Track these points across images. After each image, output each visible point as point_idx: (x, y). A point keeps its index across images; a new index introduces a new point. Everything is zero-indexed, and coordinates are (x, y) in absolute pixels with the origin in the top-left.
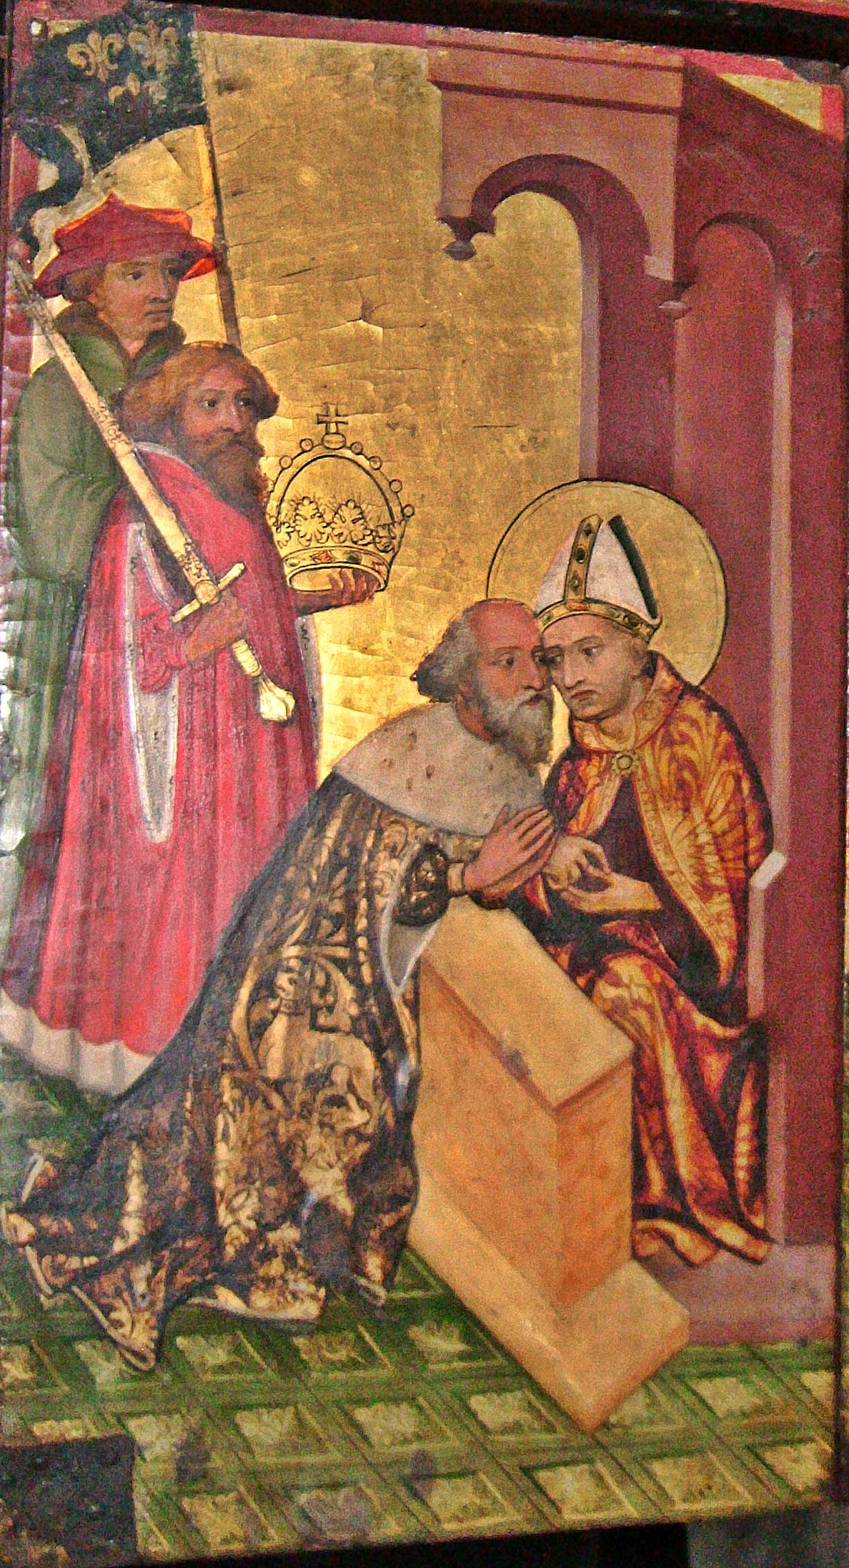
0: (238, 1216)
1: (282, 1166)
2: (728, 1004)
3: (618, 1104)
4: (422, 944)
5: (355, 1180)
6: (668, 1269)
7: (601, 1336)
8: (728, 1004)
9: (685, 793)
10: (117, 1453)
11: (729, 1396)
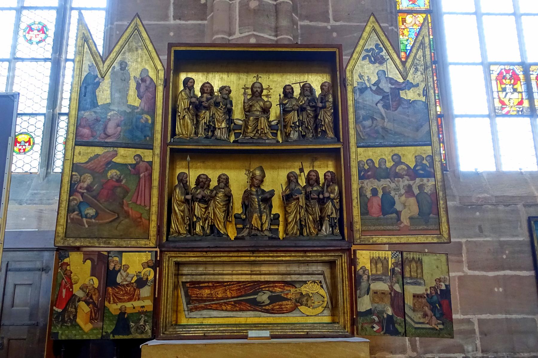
0: (66, 319)
1: (69, 316)
2: (97, 307)
3: (89, 313)
4: (78, 303)
5: (73, 317)
6: (92, 323)
7: (87, 327)
8: (97, 307)
9: (95, 295)
10: (58, 333)
11: (95, 331)
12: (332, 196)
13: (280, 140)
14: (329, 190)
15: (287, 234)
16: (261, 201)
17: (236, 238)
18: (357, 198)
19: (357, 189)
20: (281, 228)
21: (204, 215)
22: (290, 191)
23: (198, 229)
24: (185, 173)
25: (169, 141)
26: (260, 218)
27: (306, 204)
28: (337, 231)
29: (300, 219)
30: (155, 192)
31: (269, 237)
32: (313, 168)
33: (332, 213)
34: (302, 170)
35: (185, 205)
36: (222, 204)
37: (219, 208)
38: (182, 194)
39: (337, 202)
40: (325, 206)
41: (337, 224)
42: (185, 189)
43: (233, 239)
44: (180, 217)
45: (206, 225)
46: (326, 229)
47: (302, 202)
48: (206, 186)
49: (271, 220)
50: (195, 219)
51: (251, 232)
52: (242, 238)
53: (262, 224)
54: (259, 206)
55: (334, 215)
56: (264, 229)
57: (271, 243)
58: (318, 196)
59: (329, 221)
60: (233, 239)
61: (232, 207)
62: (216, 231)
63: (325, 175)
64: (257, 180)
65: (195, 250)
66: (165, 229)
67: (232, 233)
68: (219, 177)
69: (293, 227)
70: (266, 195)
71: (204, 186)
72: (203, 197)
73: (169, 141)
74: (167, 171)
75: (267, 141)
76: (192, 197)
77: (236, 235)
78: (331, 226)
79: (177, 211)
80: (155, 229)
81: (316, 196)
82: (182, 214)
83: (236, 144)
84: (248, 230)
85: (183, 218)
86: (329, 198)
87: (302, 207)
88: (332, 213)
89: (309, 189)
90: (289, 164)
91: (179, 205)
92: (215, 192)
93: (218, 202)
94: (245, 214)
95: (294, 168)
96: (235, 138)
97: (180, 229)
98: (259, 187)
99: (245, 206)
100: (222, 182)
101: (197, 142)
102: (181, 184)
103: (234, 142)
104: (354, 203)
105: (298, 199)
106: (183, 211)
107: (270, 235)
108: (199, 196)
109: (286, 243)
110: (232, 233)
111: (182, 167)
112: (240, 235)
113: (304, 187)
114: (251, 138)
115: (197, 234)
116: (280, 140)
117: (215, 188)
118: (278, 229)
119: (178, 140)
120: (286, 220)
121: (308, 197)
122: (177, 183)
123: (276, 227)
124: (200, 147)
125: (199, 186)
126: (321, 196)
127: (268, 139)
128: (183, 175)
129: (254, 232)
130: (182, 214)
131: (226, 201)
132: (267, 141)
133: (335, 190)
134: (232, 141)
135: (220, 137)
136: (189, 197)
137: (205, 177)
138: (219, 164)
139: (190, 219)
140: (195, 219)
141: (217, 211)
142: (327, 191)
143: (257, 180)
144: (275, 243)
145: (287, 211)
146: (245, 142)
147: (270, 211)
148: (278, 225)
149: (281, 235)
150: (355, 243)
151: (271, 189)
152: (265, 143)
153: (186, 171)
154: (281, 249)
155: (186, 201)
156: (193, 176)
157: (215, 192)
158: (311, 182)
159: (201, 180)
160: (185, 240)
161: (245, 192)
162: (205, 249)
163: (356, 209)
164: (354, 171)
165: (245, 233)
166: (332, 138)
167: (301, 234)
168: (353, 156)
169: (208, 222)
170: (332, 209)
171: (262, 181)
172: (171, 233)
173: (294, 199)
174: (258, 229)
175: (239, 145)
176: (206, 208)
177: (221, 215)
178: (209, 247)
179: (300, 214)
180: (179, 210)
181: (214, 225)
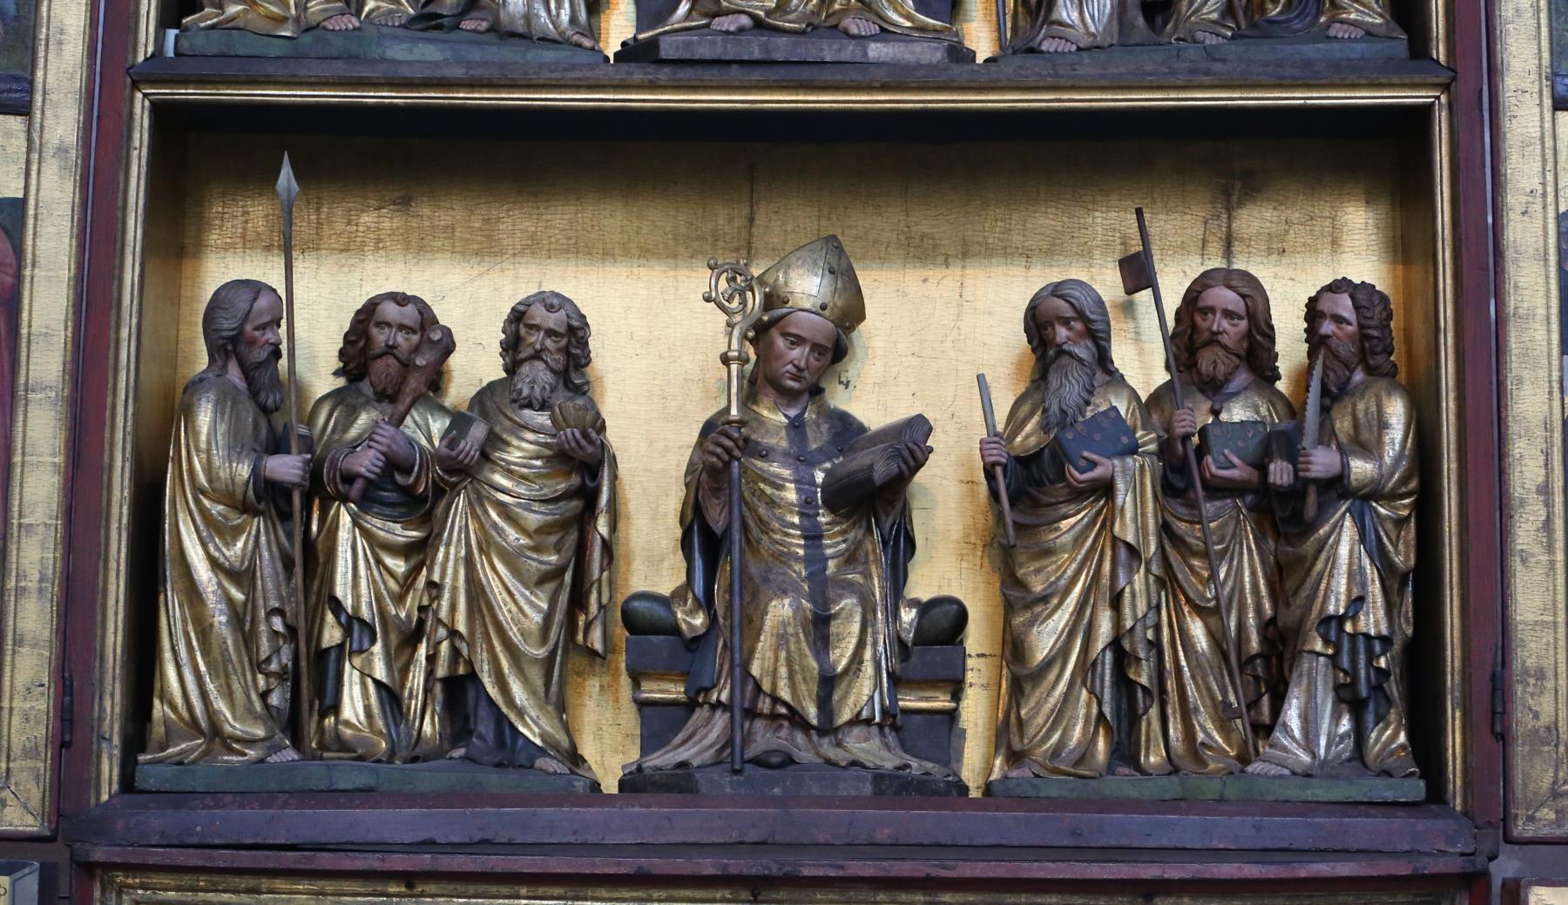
12: (1361, 468)
13: (980, 38)
14: (1343, 425)
15: (1015, 758)
16: (831, 504)
17: (633, 783)
18: (1545, 490)
19: (1547, 427)
20: (976, 710)
21: (399, 599)
22: (1045, 427)
23: (354, 703)
24: (256, 288)
25: (145, 47)
26: (820, 627)
27: (1165, 529)
28: (1390, 737)
29: (1115, 644)
30: (41, 431)
31: (879, 777)
32: (1228, 253)
33: (1356, 603)
34: (1136, 271)
35: (258, 523)
36: (533, 519)
37: (510, 558)
38: (236, 447)
39: (1400, 523)
40: (1309, 546)
41: (1393, 688)
42: (265, 410)
43: (610, 786)
44: (220, 619)
45: (417, 679)
46: (1309, 723)
47: (1135, 510)
48: (414, 383)
49: (902, 648)
50: (332, 634)
51: (747, 740)
52: (680, 782)
53: (828, 683)
54: (813, 537)
55: (1373, 620)
56: (845, 715)
57: (889, 822)
58: (1262, 468)
59: (1334, 659)
60: (610, 786)
61: (607, 547)
62: (485, 727)
63: (1314, 313)
64: (798, 340)
65: (325, 861)
66: (112, 704)
67: (608, 741)
68: (518, 317)
69: (1066, 696)
70: (862, 459)
71: (403, 380)
72: (394, 465)
73: (145, 47)
74: (131, 275)
75: (876, 51)
76: (314, 472)
77: (634, 754)
78: (1349, 699)
79: (203, 572)
80: (41, 705)
81: (1239, 472)
82: (238, 596)
83: (638, 74)
84: (721, 720)
85: (238, 616)
86: (1337, 487)
87: (1133, 552)
88: (1356, 603)
89: (1196, 414)
90: (1046, 220)
91: (214, 529)
92: (478, 431)
93: (502, 508)
94: (707, 603)
95: (1085, 255)
96: (640, 28)
97: (220, 705)
98: (816, 391)
99: (704, 537)
100: (537, 356)
101: (352, 58)
102: (234, 374)
103: (629, 52)
104: (1526, 532)
105: (1105, 489)
106: (242, 576)
107: (889, 761)
108: (366, 462)
109: (1010, 825)
110: (608, 741)
111: (247, 242)
112: (663, 759)
113: (1157, 396)
114: (759, 24)
115: (342, 745)
116: (980, 38)
117: (486, 397)
118: (952, 716)
119: (214, 44)
120: (1013, 648)
121: (1179, 474)
122: (203, 361)
123: (942, 702)
124: (371, 97)
125: (366, 387)
126: (1280, 473)
127: (886, 33)
128: (242, 301)
129: (764, 738)
130: (238, 596)
131: (566, 496)
132: (876, 51)
133: (1383, 425)
134: (612, 47)
135: (528, 17)
136: (287, 467)
137: (409, 314)
138: (516, 220)
139: (292, 630)
140: (332, 634)
141: (497, 578)
142: (1326, 435)
143: (798, 340)
144: (923, 821)
145: (1021, 584)
146: (705, 52)
147: (897, 578)
148: (957, 688)
149: (975, 760)
150: (1522, 829)
151: (901, 411)
152: (865, 65)
153: (269, 272)
154: (966, 870)
155: (268, 498)
156: (321, 305)
157: (478, 431)
158: (1207, 361)
159: (381, 337)
160: (258, 790)
161: (708, 428)
162: (398, 862)
163: (1538, 574)
164: (1532, 288)
165: (698, 744)
166: (1370, 34)
167: (1126, 752)
168: (1523, 171)
169: (432, 659)
170: (1356, 575)
171: (836, 351)
172: (158, 730)
173: (1079, 495)
174: (796, 718)
175: (664, 74)
176: (419, 552)
177: (523, 609)
178: (428, 845)
179: (1116, 603)
180: (215, 564)
181: (473, 676)
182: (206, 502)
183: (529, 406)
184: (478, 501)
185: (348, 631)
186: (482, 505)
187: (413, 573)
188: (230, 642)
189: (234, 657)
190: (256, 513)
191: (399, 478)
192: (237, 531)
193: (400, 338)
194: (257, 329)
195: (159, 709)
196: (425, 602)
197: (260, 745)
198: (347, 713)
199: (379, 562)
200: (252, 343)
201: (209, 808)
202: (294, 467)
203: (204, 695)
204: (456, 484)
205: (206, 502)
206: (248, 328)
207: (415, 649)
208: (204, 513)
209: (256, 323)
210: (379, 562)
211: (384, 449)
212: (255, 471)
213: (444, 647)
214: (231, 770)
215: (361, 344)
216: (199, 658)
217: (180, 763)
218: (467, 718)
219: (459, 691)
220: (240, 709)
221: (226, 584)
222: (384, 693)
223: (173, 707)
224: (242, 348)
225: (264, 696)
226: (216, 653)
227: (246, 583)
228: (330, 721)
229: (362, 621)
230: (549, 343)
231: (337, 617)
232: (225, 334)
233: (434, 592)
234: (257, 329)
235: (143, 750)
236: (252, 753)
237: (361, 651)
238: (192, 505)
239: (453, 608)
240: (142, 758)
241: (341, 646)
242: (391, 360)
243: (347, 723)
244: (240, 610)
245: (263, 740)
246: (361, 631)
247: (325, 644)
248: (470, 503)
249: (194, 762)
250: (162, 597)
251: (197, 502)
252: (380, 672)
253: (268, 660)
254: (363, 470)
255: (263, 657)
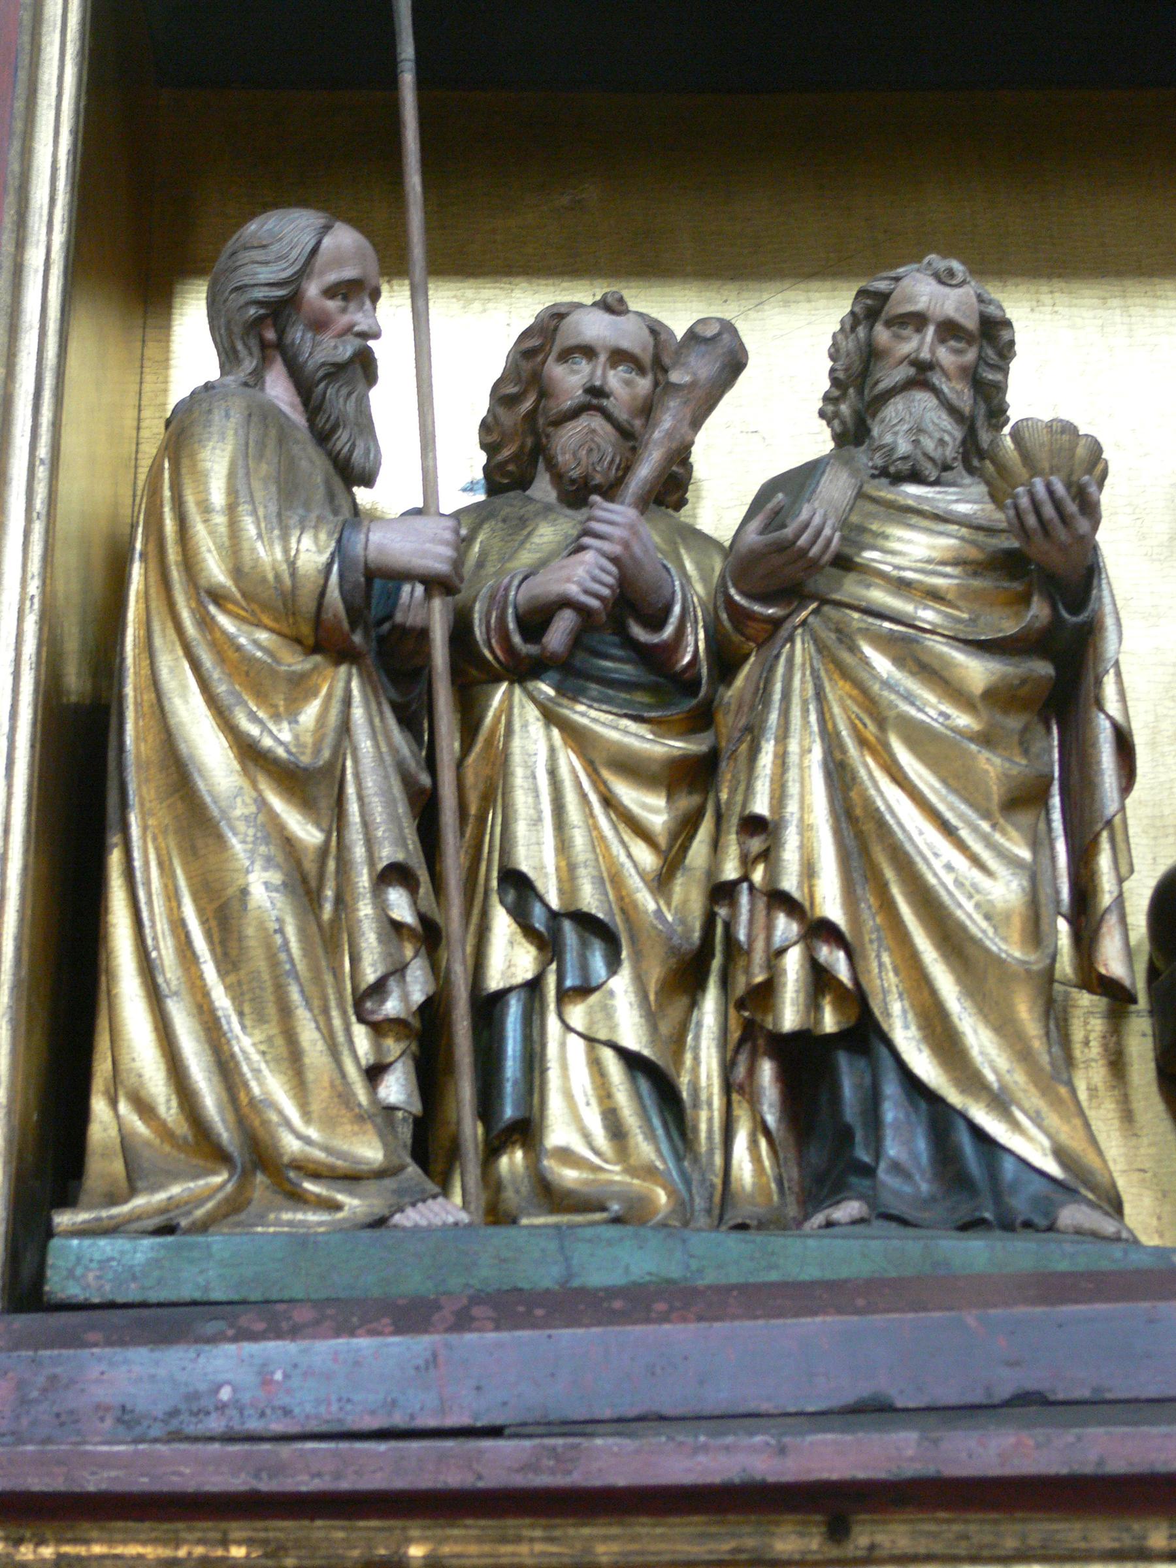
23: (578, 1111)
44: (262, 889)
50: (510, 958)
62: (902, 1143)
85: (305, 883)
91: (235, 682)
97: (270, 1085)
100: (922, 375)
102: (278, 389)
130: (307, 832)
159: (570, 380)
180: (250, 754)
181: (865, 1033)
182: (223, 620)
183: (916, 477)
184: (837, 656)
185: (548, 944)
186: (854, 649)
187: (686, 827)
188: (291, 931)
189: (301, 966)
190: (342, 654)
191: (639, 633)
192: (299, 688)
193: (615, 379)
194: (330, 292)
195: (104, 1119)
196: (730, 871)
197: (372, 1186)
198: (559, 1132)
199: (609, 802)
200: (319, 324)
201: (254, 1337)
202: (434, 540)
203: (226, 1067)
204: (776, 623)
205: (223, 620)
206: (313, 290)
207: (695, 1003)
208: (223, 646)
209: (332, 277)
210: (609, 802)
211: (615, 549)
212: (340, 550)
213: (793, 961)
214: (302, 1241)
215: (527, 405)
216: (209, 971)
217: (169, 1229)
218: (845, 1135)
219: (823, 1077)
220: (320, 1097)
221: (277, 803)
222: (644, 1085)
223: (144, 1108)
224: (298, 334)
225: (374, 1073)
226: (258, 961)
227: (326, 805)
228: (513, 1161)
229: (587, 922)
230: (944, 355)
231: (520, 915)
232: (260, 294)
233: (756, 845)
234: (330, 292)
235: (67, 1199)
236: (353, 1204)
237: (585, 990)
238: (191, 629)
239: (809, 871)
240: (63, 1219)
241: (534, 986)
242: (596, 422)
243: (566, 1155)
244: (310, 866)
245: (380, 1174)
246: (584, 945)
247: (495, 981)
248: (821, 648)
249: (203, 1227)
250: (115, 858)
251: (206, 623)
252: (632, 1033)
253: (379, 989)
254: (573, 590)
255: (370, 975)
